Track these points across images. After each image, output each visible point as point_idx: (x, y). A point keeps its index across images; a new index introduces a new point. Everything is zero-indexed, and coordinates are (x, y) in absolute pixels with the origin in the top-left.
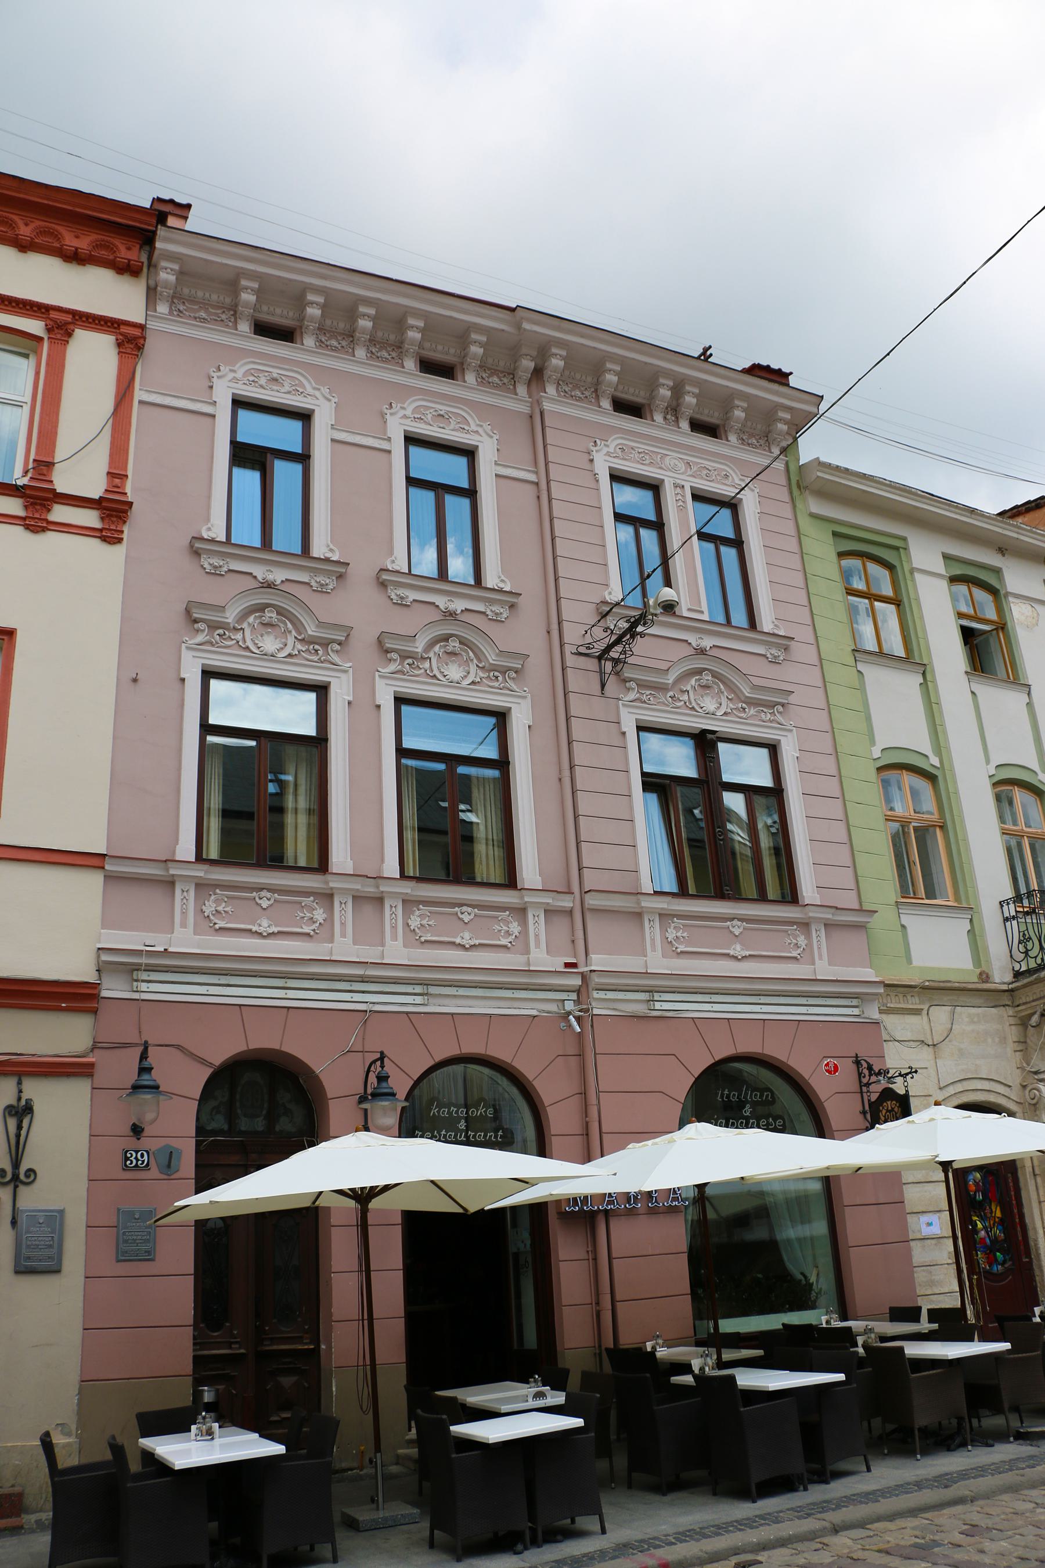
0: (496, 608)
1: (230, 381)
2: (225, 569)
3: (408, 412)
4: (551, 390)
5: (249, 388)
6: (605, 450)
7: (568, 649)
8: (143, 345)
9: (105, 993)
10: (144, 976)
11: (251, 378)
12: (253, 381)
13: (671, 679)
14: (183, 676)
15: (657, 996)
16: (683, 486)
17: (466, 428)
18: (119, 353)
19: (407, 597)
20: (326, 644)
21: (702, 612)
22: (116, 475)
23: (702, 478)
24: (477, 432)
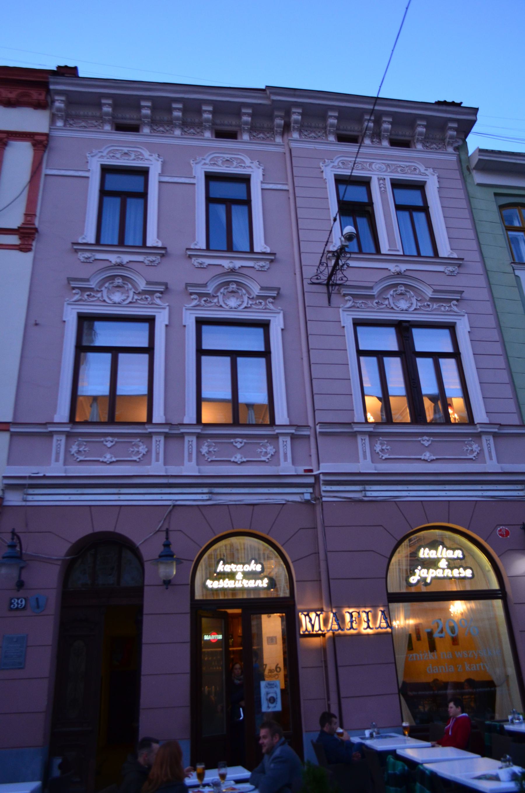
0: (262, 263)
1: (99, 158)
2: (93, 259)
3: (207, 161)
4: (295, 135)
5: (111, 160)
6: (332, 164)
7: (306, 282)
8: (47, 144)
9: (6, 503)
10: (31, 491)
11: (111, 155)
12: (113, 156)
13: (375, 292)
14: (64, 319)
15: (368, 488)
16: (385, 179)
17: (243, 165)
18: (34, 150)
19: (204, 263)
20: (152, 293)
21: (398, 251)
22: (30, 215)
23: (398, 172)
24: (250, 167)
